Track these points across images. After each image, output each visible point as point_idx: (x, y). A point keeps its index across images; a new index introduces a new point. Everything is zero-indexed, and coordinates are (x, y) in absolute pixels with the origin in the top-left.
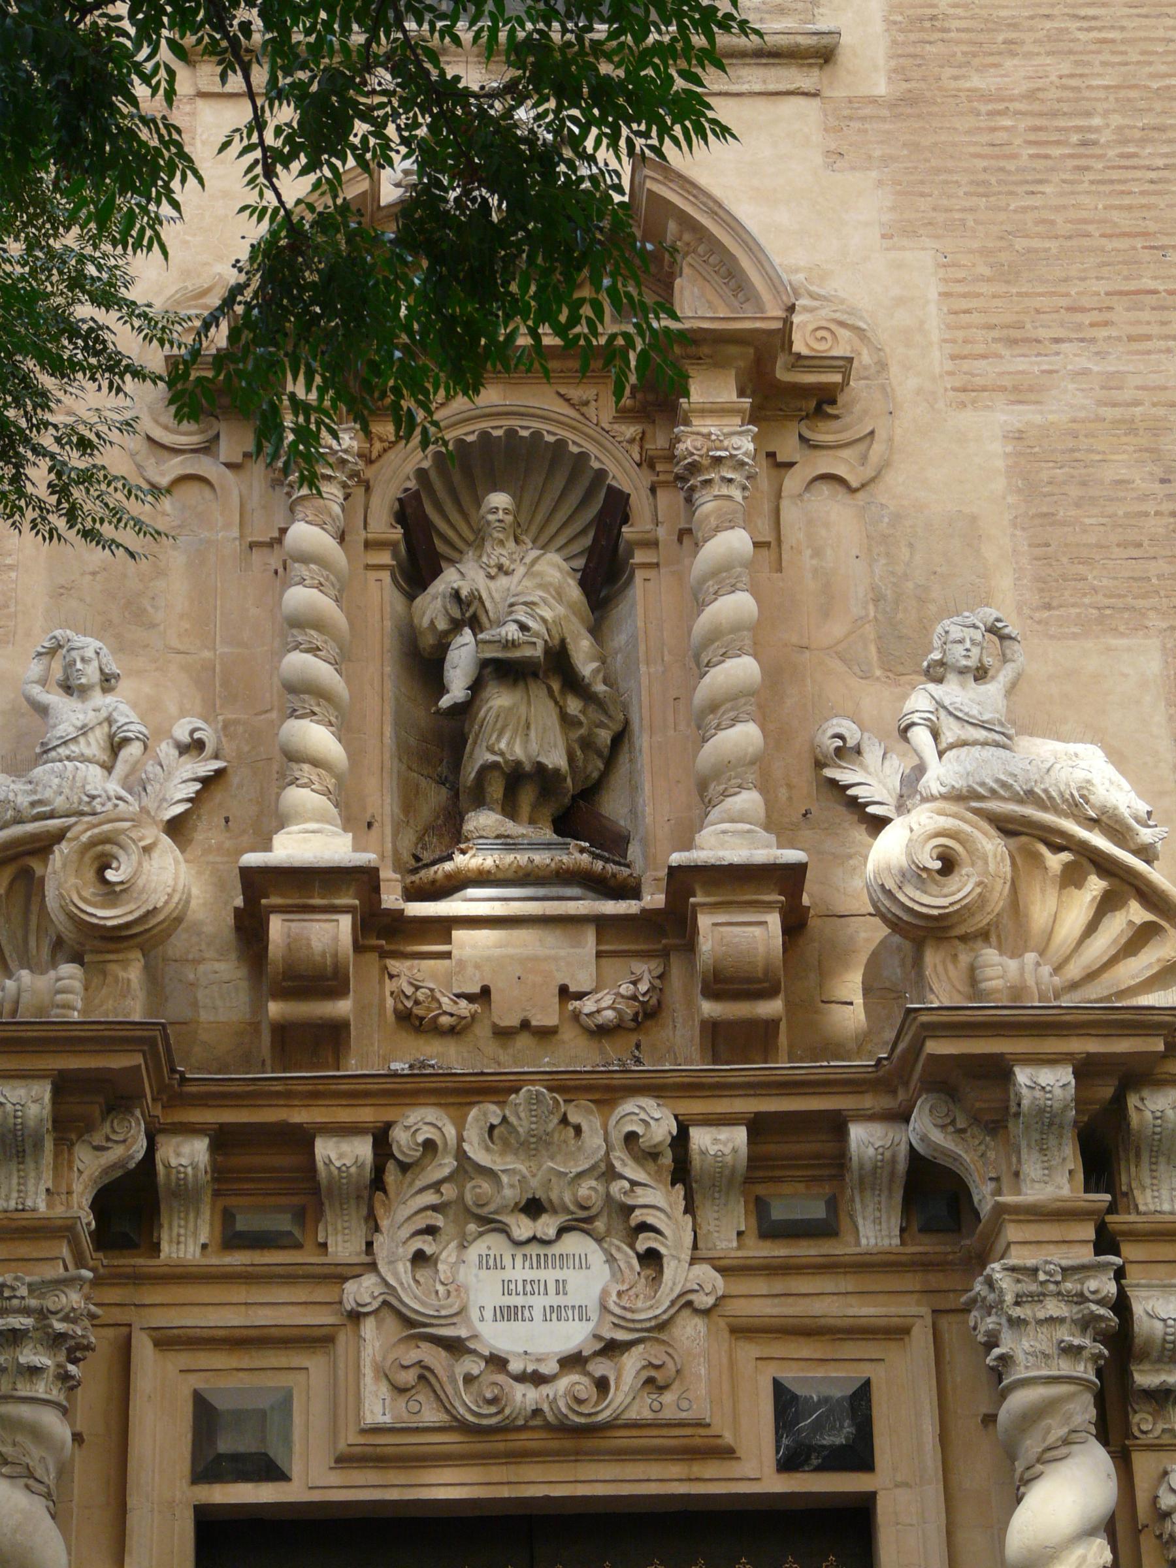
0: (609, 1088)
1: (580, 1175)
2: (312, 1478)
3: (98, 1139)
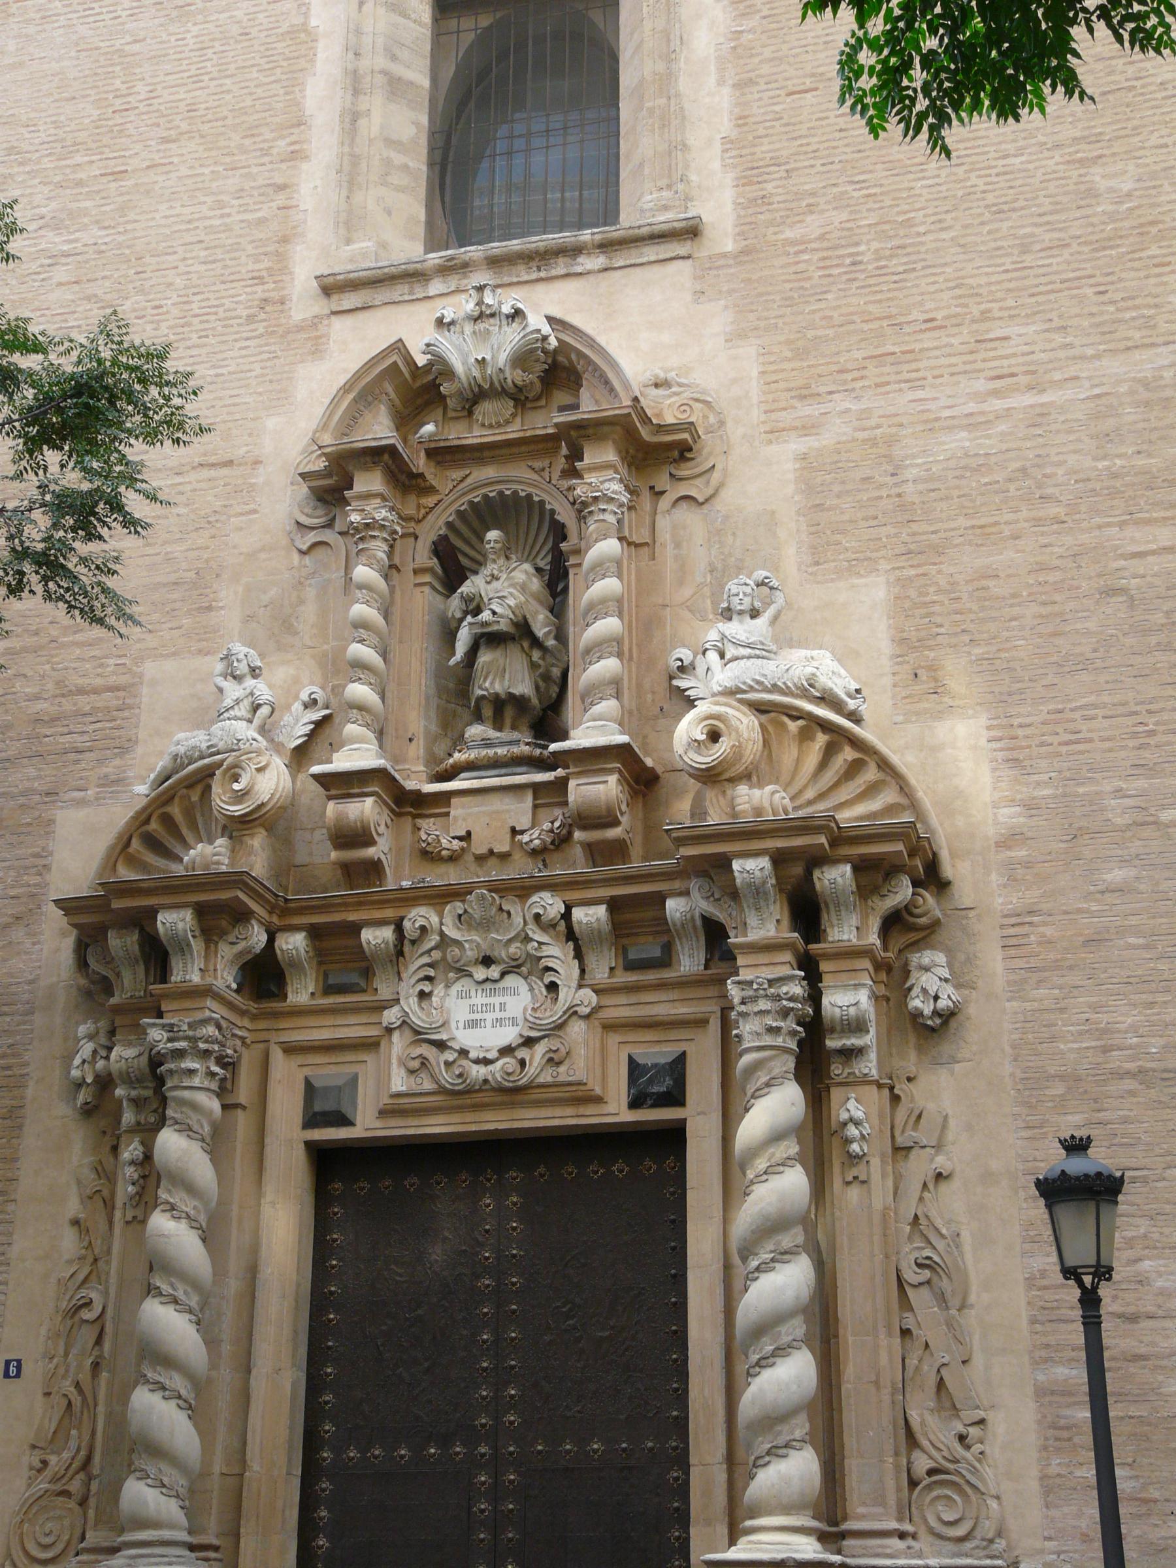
0: (523, 888)
1: (510, 941)
2: (366, 1124)
3: (231, 938)
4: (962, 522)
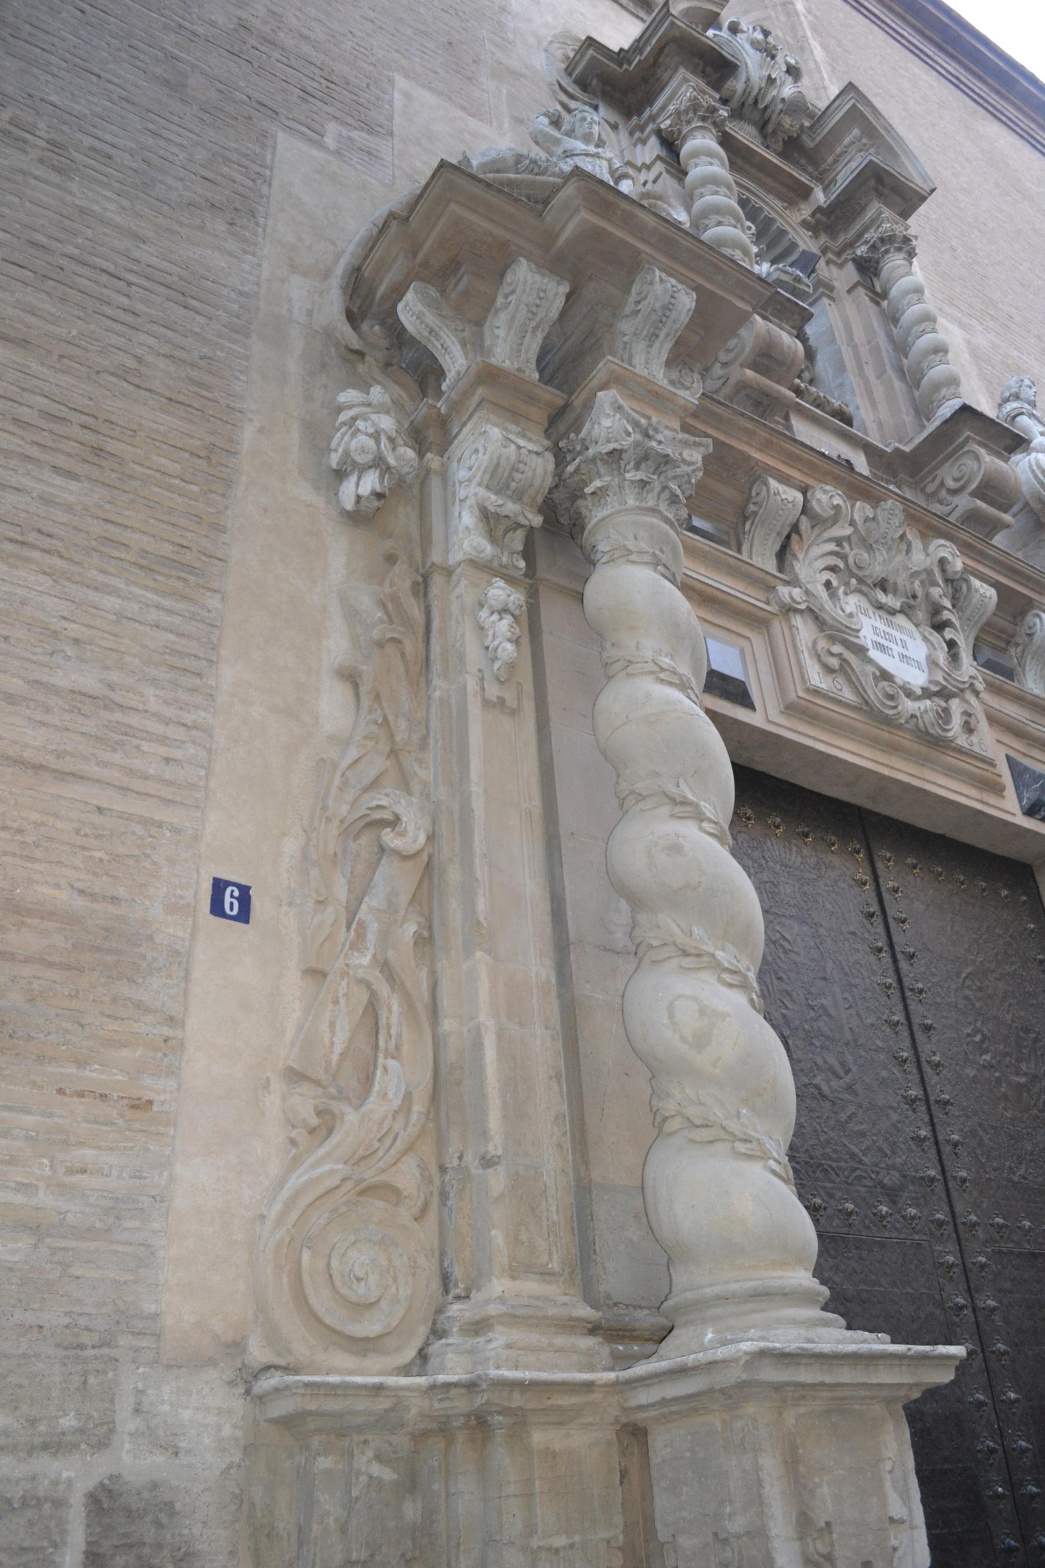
0: (929, 526)
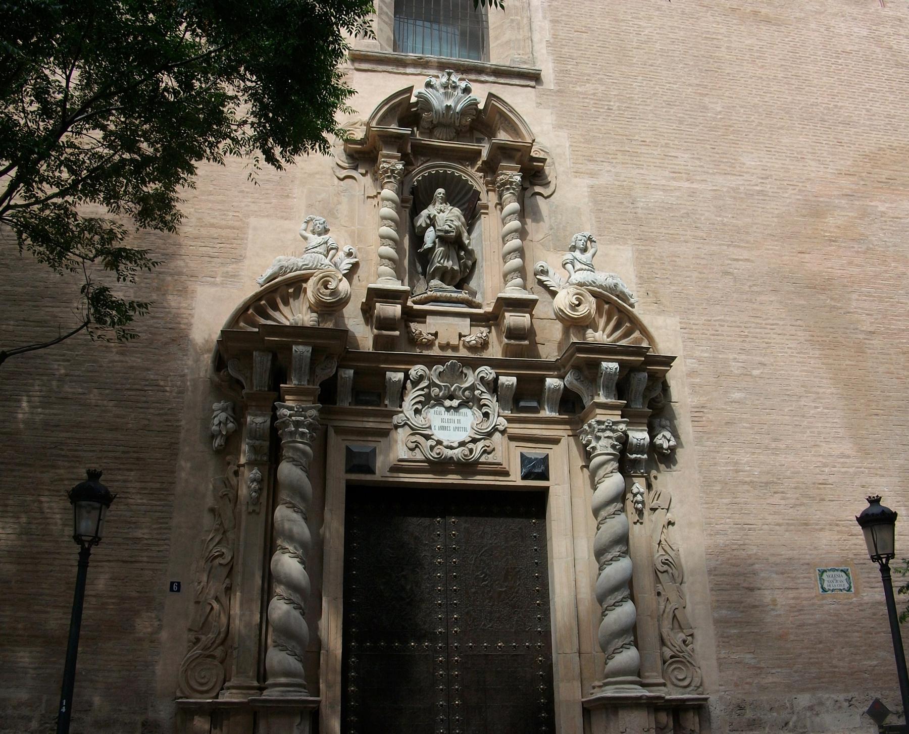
4: (662, 230)
